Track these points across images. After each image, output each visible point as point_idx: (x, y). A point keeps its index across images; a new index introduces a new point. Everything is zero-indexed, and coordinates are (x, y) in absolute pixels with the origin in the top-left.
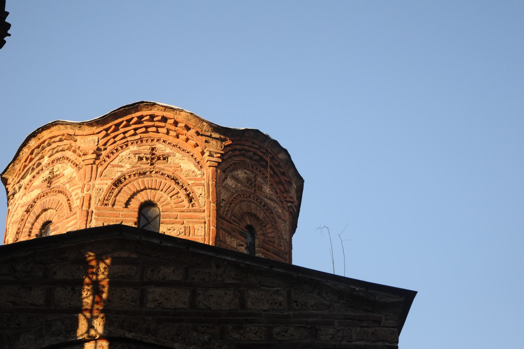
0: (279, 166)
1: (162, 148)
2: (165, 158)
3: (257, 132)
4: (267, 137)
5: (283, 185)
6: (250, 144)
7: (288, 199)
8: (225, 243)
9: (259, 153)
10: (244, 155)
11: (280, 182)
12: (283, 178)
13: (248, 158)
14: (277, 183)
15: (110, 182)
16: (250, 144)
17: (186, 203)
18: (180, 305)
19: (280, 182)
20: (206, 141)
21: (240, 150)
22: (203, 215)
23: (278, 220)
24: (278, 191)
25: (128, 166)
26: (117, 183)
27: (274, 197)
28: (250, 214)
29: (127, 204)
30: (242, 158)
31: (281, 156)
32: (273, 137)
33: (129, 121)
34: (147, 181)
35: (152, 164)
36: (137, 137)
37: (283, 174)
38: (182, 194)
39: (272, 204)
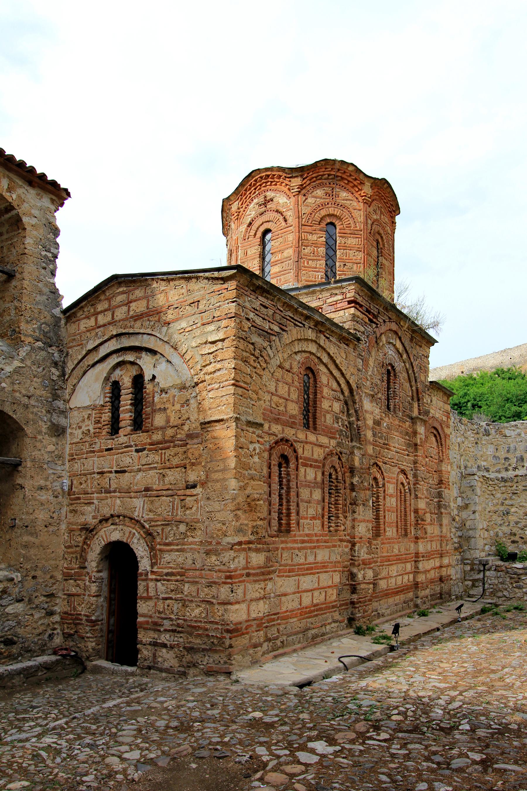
0: (351, 175)
1: (270, 194)
2: (272, 200)
3: (325, 160)
4: (334, 161)
5: (357, 187)
6: (324, 170)
7: (362, 194)
8: (307, 240)
9: (332, 173)
10: (321, 179)
11: (355, 186)
12: (355, 183)
13: (325, 179)
14: (353, 187)
15: (246, 226)
16: (324, 170)
17: (283, 224)
18: (143, 309)
19: (355, 186)
20: (290, 181)
21: (316, 177)
22: (292, 228)
23: (353, 211)
24: (354, 192)
25: (254, 213)
26: (250, 224)
27: (350, 198)
28: (330, 215)
29: (255, 234)
30: (320, 181)
31: (351, 168)
32: (339, 159)
33: (250, 185)
34: (264, 218)
35: (266, 207)
36: (257, 193)
37: (356, 179)
38: (281, 218)
39: (348, 202)
